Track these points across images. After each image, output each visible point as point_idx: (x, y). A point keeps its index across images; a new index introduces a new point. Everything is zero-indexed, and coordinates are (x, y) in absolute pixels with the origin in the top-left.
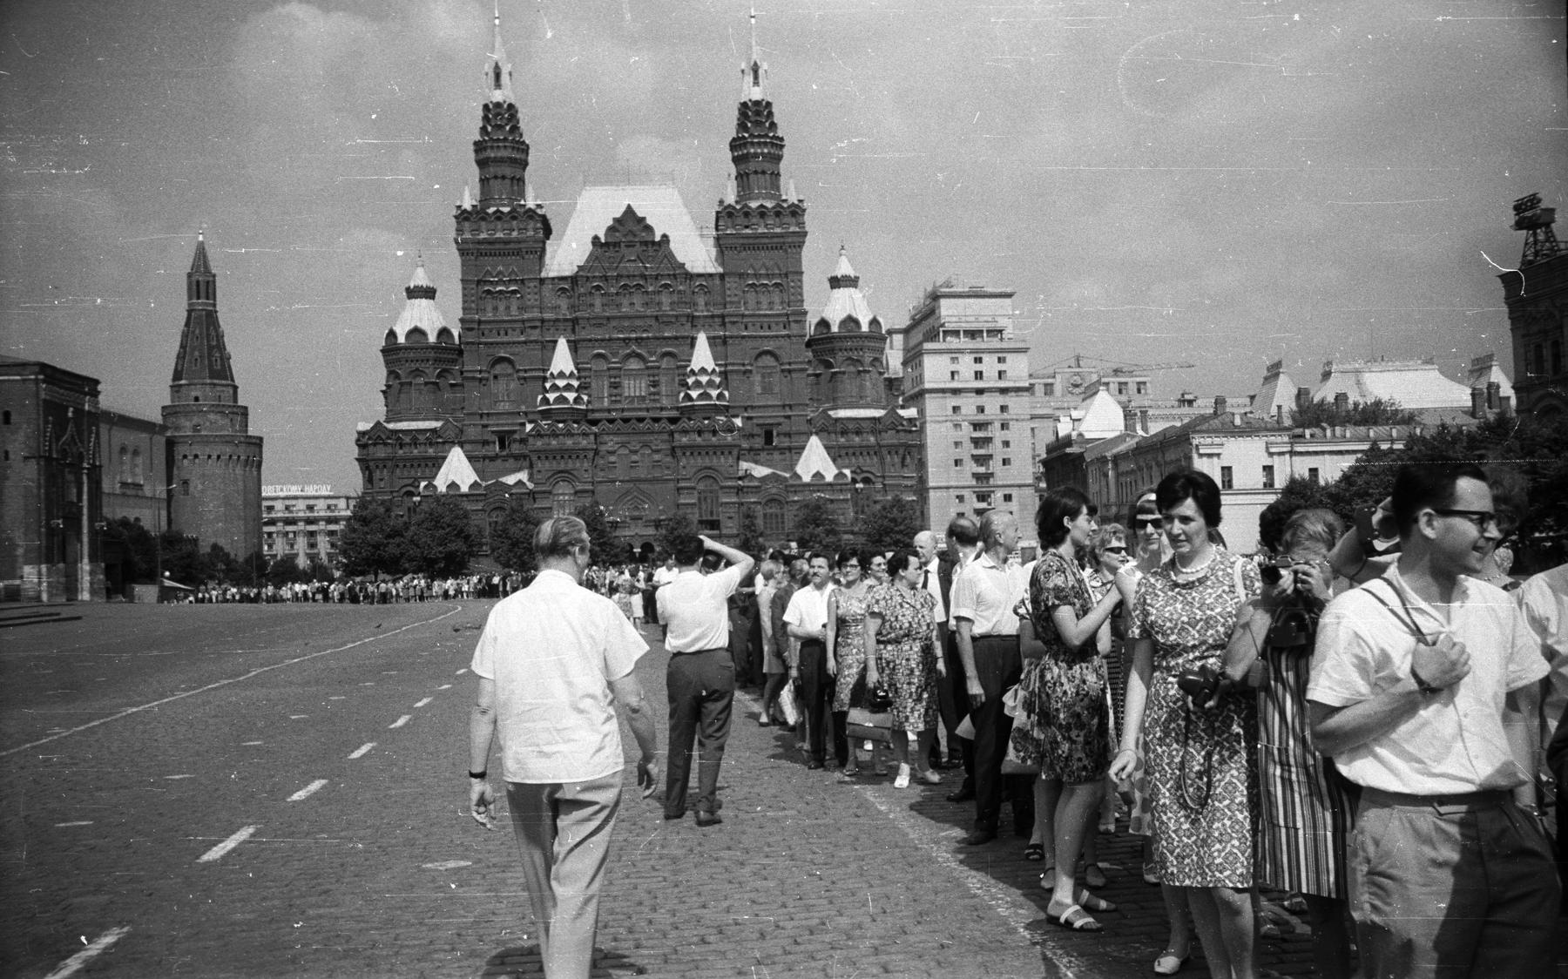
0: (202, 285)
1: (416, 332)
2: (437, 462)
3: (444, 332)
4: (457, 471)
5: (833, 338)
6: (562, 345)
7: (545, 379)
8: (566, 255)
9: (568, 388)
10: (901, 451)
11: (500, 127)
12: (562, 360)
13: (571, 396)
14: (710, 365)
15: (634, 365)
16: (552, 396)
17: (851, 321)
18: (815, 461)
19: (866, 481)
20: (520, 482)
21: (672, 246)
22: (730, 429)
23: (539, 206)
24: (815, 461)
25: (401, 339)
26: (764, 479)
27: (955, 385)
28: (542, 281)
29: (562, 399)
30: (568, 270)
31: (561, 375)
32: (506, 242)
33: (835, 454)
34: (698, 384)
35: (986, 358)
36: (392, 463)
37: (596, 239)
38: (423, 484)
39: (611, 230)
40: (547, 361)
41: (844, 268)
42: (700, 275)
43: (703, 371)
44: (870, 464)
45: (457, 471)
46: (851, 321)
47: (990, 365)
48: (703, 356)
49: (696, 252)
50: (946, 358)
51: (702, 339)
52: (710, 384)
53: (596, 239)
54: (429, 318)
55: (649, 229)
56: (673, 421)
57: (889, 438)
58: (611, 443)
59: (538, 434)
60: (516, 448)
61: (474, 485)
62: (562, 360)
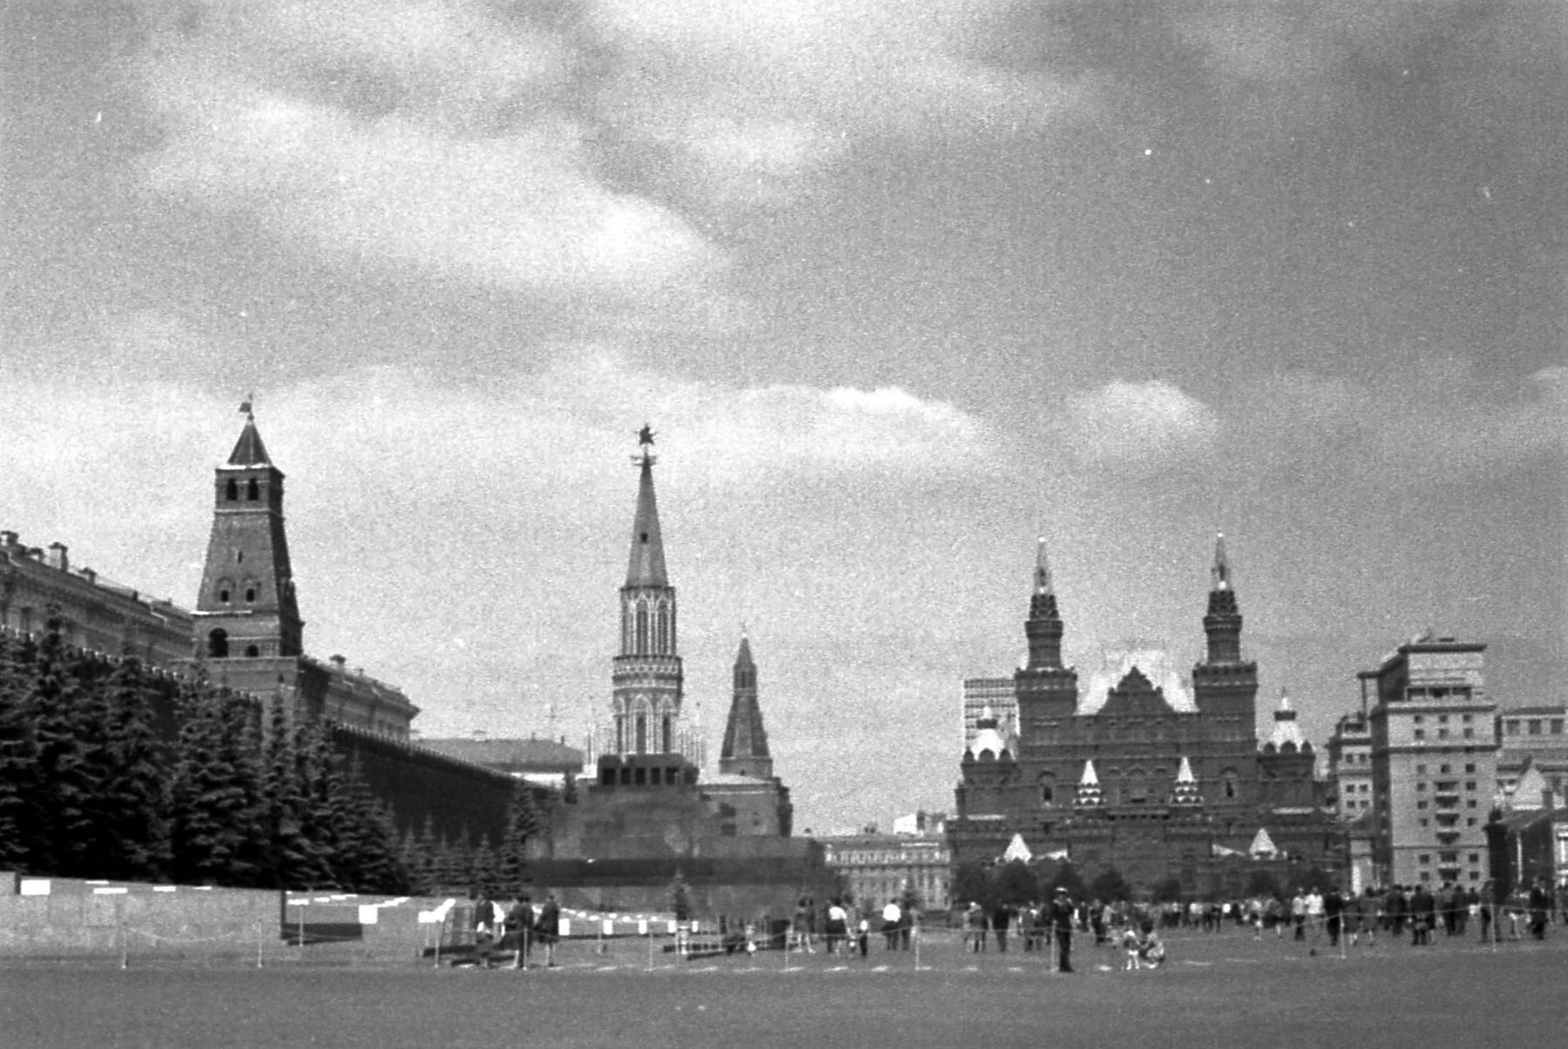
1: (987, 753)
2: (1006, 843)
6: (1089, 766)
7: (1076, 788)
11: (1043, 613)
12: (1090, 776)
13: (1096, 800)
14: (1190, 779)
15: (1137, 777)
16: (1084, 800)
17: (1289, 746)
18: (1263, 843)
19: (1299, 858)
22: (1205, 824)
24: (1263, 843)
25: (976, 758)
26: (1228, 858)
29: (1090, 803)
30: (1094, 712)
31: (1089, 786)
32: (1052, 692)
33: (1275, 838)
34: (1182, 793)
36: (972, 843)
38: (997, 859)
39: (1122, 684)
41: (1285, 705)
42: (1183, 715)
43: (1185, 783)
44: (1303, 847)
45: (1018, 850)
46: (1289, 746)
48: (1186, 774)
49: (1180, 699)
51: (1185, 761)
52: (1191, 792)
54: (991, 741)
55: (1148, 683)
56: (1166, 817)
57: (1318, 829)
58: (1123, 832)
59: (1075, 826)
60: (1056, 834)
61: (1032, 860)
62: (1090, 776)
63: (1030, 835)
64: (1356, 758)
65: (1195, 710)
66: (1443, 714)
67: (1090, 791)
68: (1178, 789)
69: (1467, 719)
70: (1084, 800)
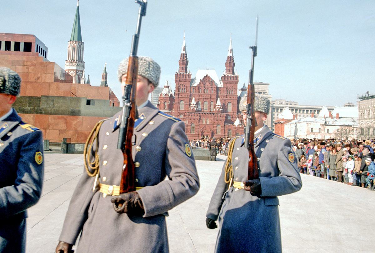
6: (194, 99)
37: (201, 80)
40: (190, 102)
68: (217, 107)
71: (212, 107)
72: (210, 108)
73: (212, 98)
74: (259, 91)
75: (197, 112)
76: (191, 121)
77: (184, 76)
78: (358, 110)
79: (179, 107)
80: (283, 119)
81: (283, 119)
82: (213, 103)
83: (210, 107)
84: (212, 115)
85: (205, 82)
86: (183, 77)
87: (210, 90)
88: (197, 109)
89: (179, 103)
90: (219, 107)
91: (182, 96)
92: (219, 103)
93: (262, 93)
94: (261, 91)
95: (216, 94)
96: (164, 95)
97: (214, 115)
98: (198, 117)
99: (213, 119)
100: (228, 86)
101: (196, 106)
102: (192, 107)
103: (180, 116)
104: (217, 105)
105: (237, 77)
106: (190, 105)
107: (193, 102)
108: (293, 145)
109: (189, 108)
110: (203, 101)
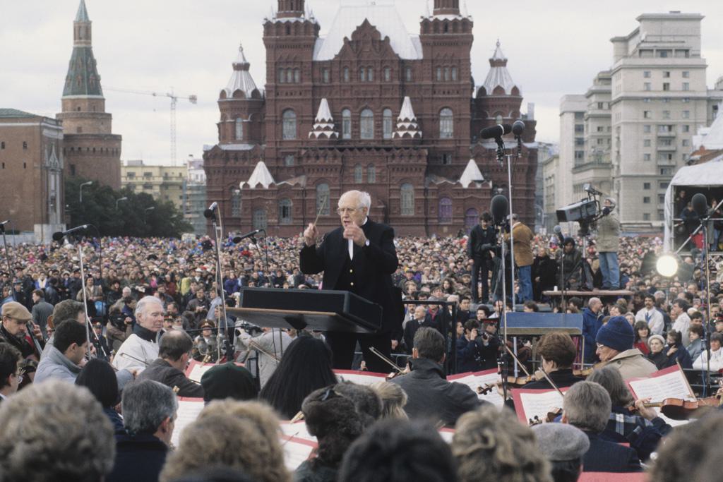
0: (83, 30)
2: (248, 172)
3: (256, 92)
4: (261, 176)
5: (488, 99)
6: (324, 102)
8: (328, 48)
9: (327, 129)
10: (526, 170)
13: (328, 134)
20: (297, 185)
21: (392, 43)
23: (313, 18)
27: (647, 94)
28: (314, 63)
35: (672, 73)
37: (346, 39)
38: (242, 184)
39: (354, 34)
40: (315, 111)
47: (676, 80)
49: (407, 45)
50: (641, 73)
52: (411, 128)
53: (346, 39)
55: (378, 34)
61: (271, 185)
63: (274, 164)
64: (442, 92)
65: (421, 56)
66: (647, 70)
67: (323, 126)
68: (399, 125)
69: (685, 75)
70: (317, 134)
71: (387, 124)
72: (380, 130)
73: (387, 96)
74: (660, 46)
75: (332, 146)
76: (314, 176)
77: (292, 31)
78: (166, 162)
79: (279, 132)
80: (702, 147)
81: (702, 147)
82: (388, 113)
83: (379, 126)
84: (385, 153)
85: (361, 44)
86: (288, 33)
87: (378, 69)
88: (333, 136)
89: (279, 119)
90: (407, 125)
91: (287, 94)
92: (407, 111)
93: (671, 51)
94: (667, 45)
95: (397, 82)
96: (231, 96)
97: (390, 154)
98: (336, 162)
99: (388, 166)
100: (438, 55)
101: (332, 126)
102: (319, 129)
103: (284, 159)
104: (400, 121)
105: (466, 25)
106: (314, 123)
107: (324, 112)
108: (589, 238)
109: (310, 133)
110: (357, 107)
